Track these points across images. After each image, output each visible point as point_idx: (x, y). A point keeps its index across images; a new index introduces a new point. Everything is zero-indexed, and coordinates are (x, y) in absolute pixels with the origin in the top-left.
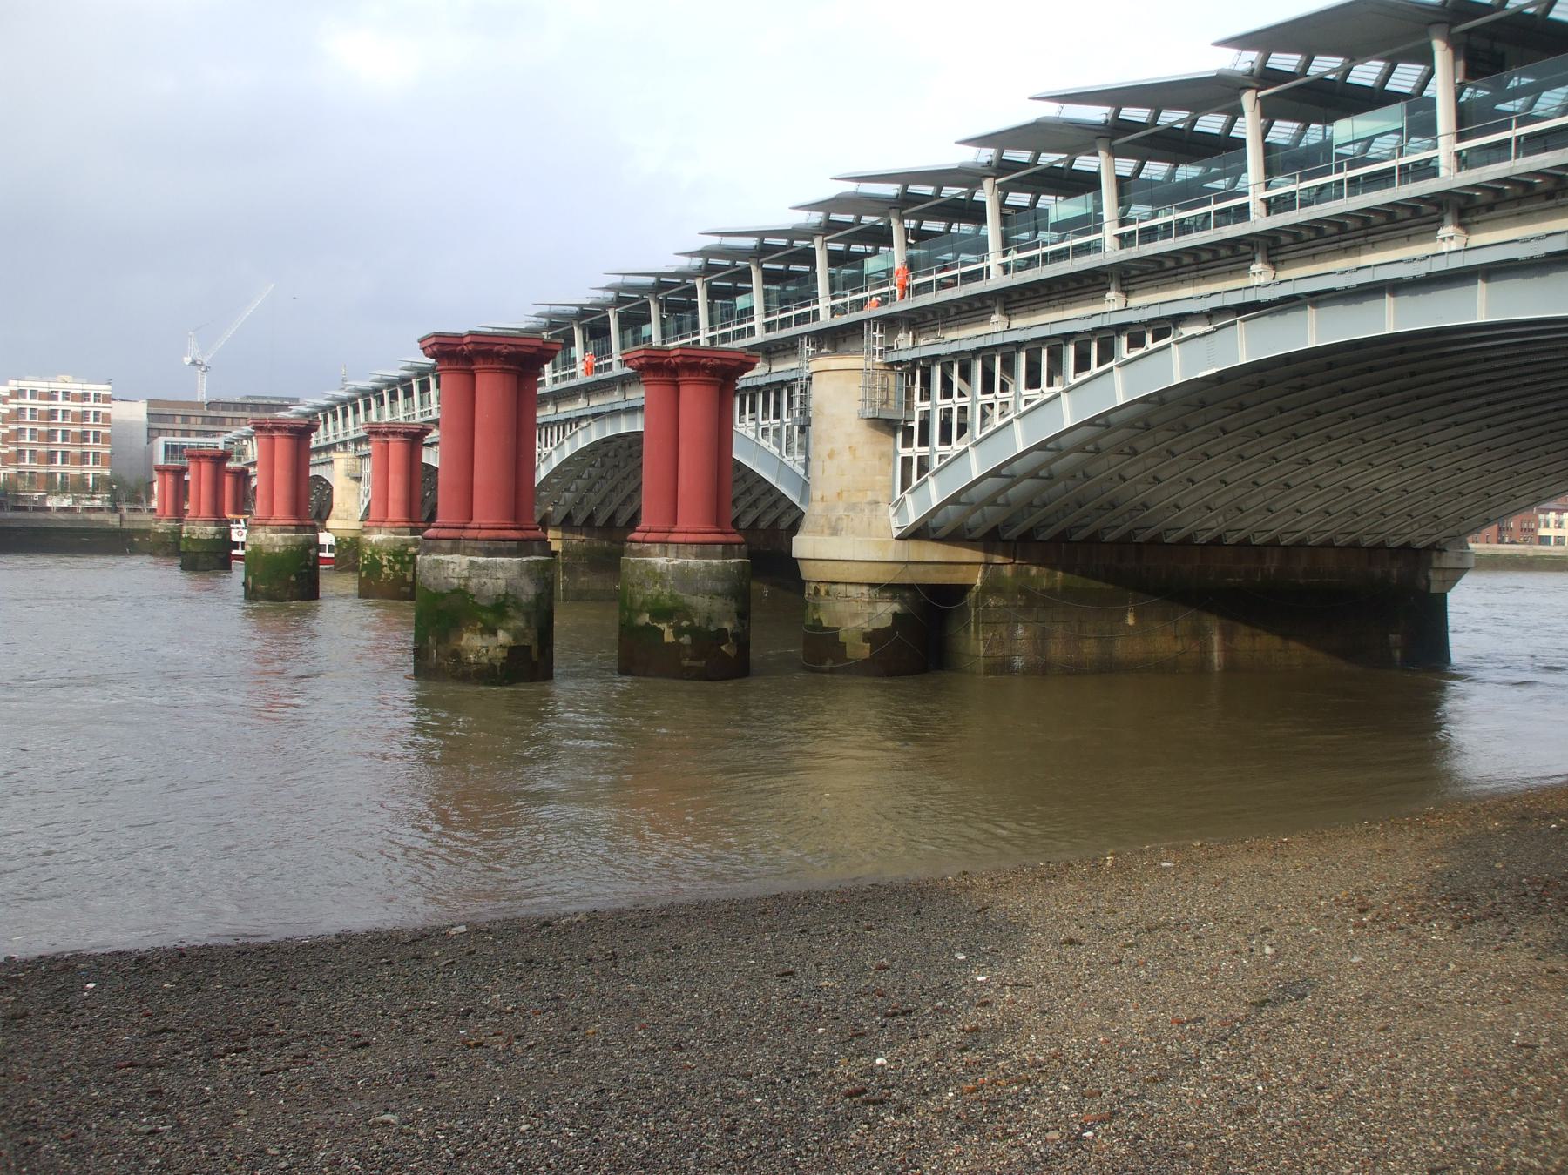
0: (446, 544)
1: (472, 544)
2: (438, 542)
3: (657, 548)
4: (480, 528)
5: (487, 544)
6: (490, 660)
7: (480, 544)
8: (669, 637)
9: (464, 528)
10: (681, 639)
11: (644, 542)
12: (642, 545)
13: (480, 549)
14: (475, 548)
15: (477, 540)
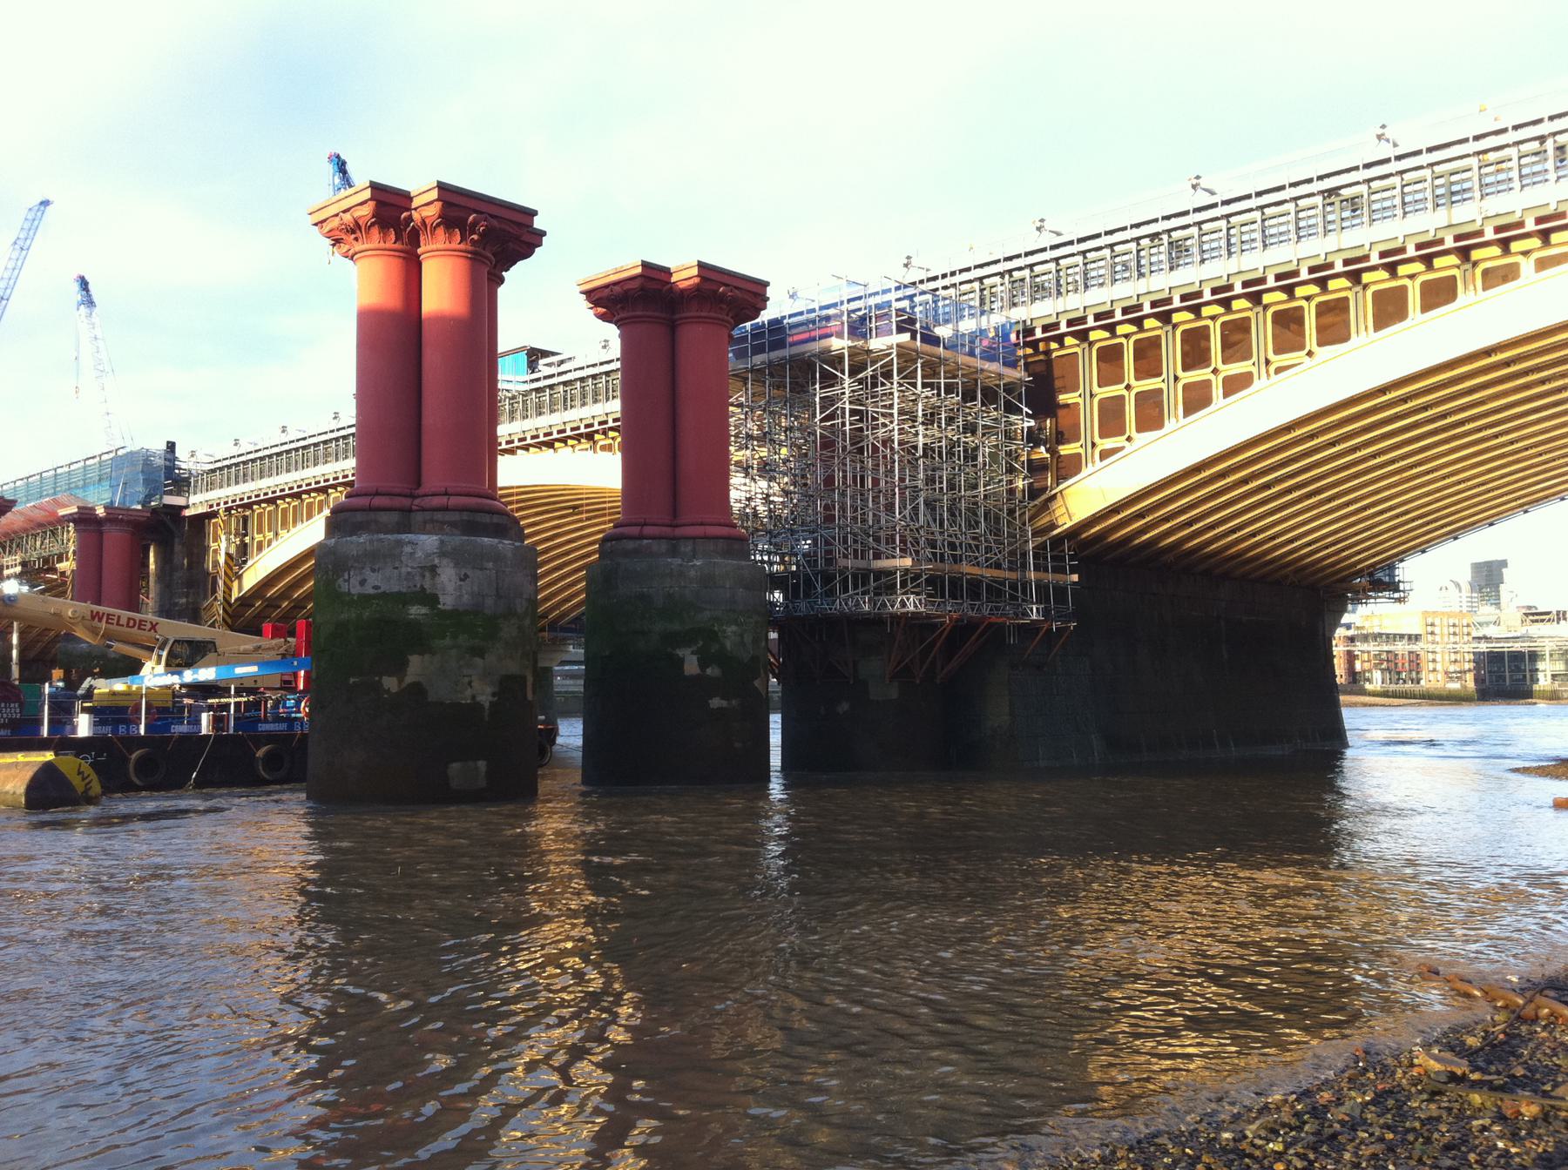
0: (394, 517)
1: (439, 516)
2: (372, 515)
3: (663, 546)
4: (446, 494)
5: (465, 516)
6: (473, 697)
7: (455, 516)
8: (691, 666)
9: (414, 497)
10: (709, 671)
11: (641, 537)
12: (638, 542)
13: (453, 524)
14: (443, 523)
15: (446, 509)
